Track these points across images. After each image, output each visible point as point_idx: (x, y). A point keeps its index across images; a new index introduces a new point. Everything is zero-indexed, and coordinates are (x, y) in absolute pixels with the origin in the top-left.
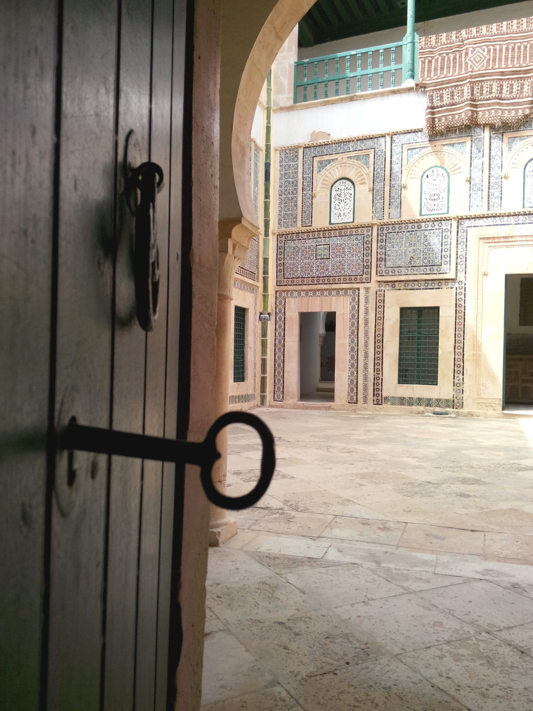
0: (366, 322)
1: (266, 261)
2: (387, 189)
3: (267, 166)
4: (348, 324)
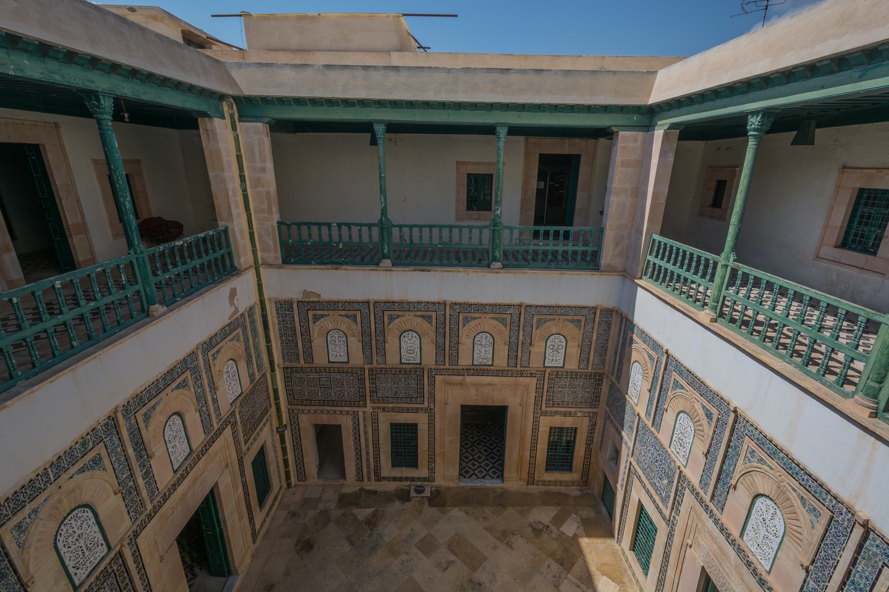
0: (366, 433)
1: (276, 391)
2: (374, 343)
3: (264, 317)
4: (352, 433)
